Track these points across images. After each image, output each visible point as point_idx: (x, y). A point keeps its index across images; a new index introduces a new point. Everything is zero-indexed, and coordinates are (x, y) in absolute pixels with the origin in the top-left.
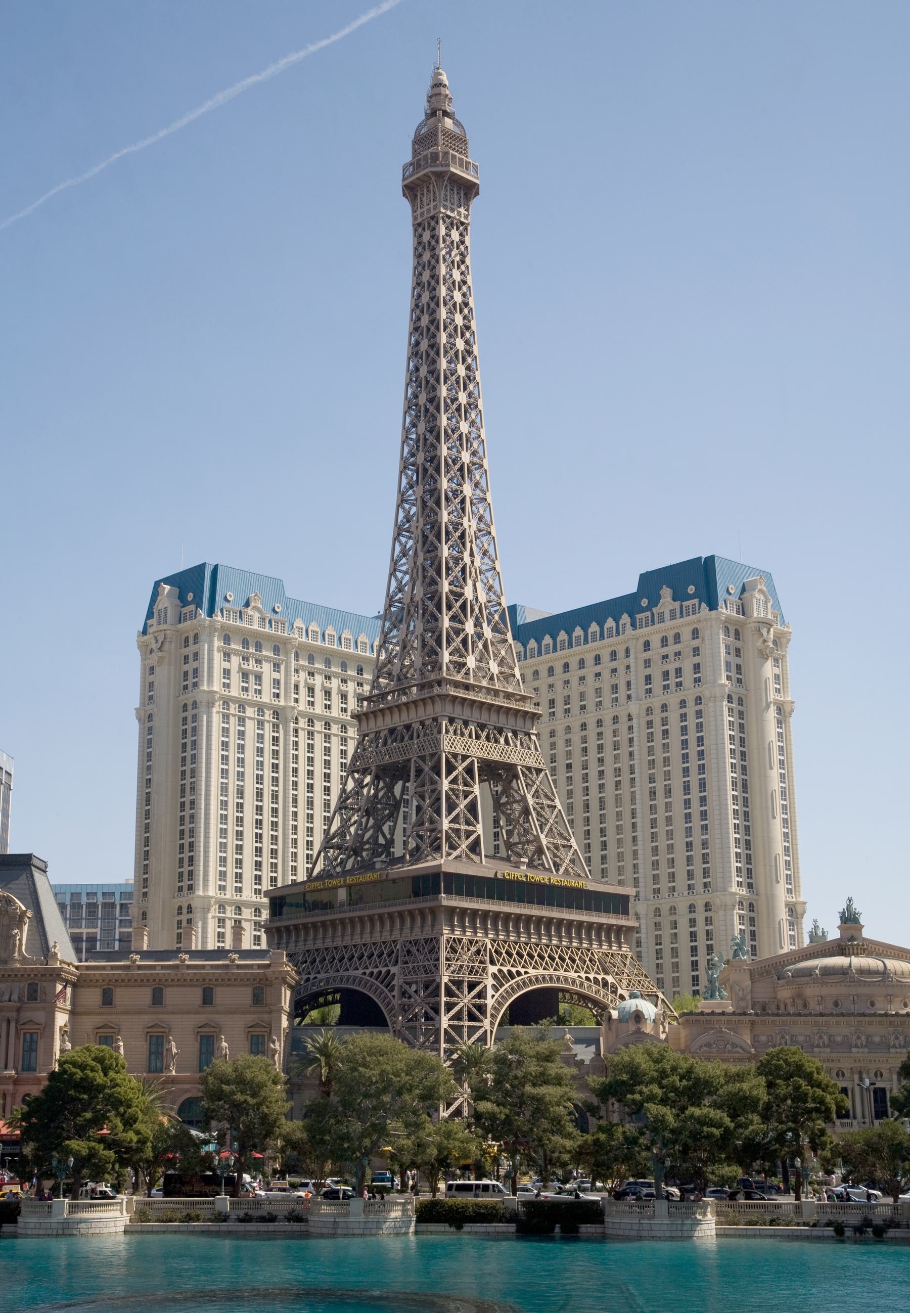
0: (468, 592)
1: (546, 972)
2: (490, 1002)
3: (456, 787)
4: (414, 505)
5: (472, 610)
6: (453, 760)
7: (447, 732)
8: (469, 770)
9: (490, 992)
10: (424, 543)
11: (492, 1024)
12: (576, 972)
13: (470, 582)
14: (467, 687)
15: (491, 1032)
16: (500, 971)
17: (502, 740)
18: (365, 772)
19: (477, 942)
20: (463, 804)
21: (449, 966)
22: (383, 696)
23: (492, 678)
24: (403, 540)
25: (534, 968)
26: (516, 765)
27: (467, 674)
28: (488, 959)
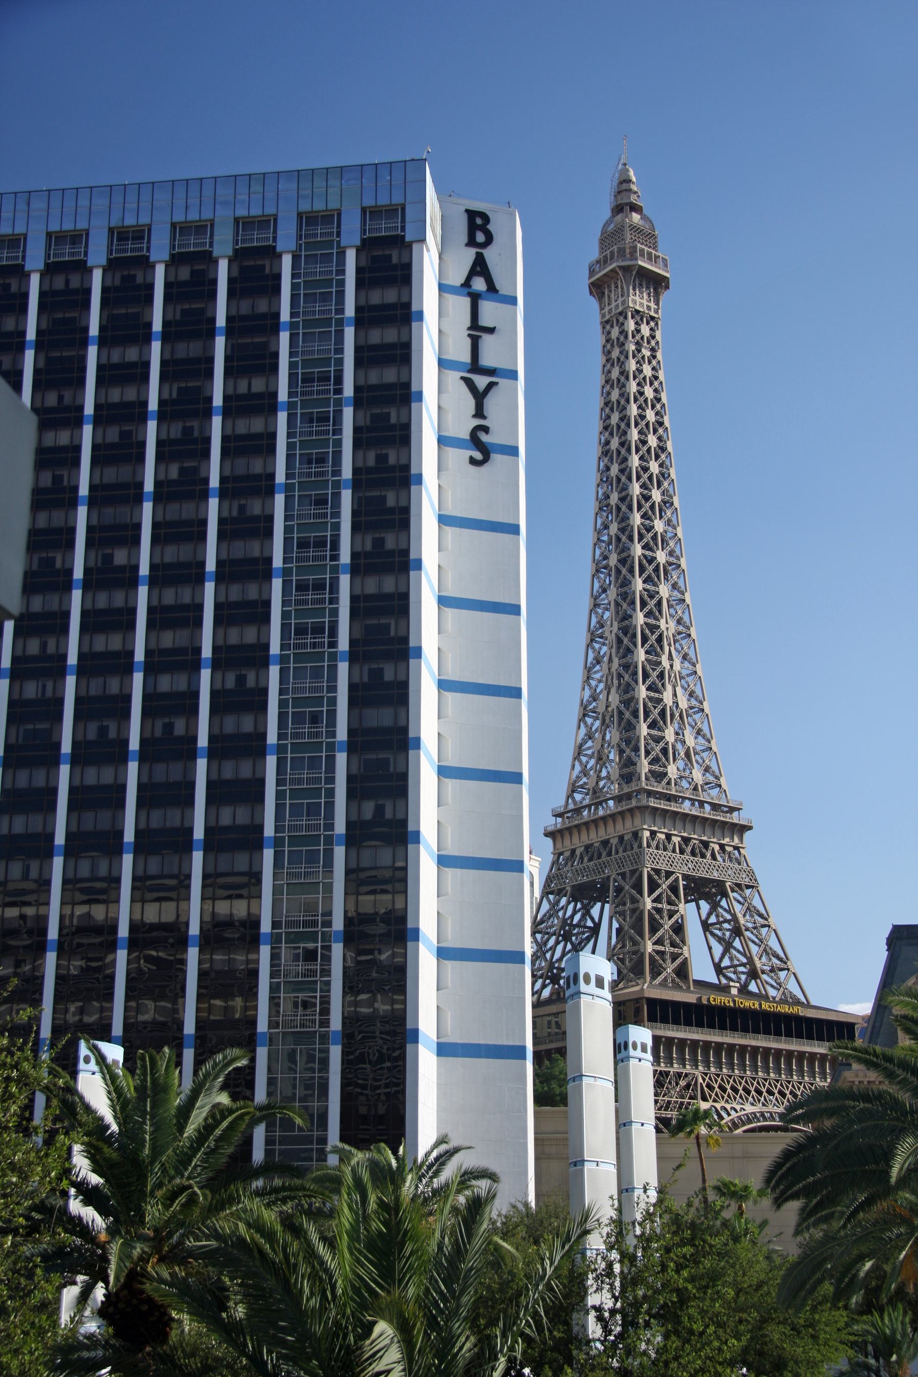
1: (764, 1109)
3: (660, 906)
4: (607, 609)
6: (656, 877)
7: (649, 846)
8: (674, 888)
10: (618, 648)
13: (669, 688)
14: (669, 798)
17: (708, 854)
18: (560, 893)
20: (668, 924)
22: (578, 811)
23: (695, 789)
24: (597, 646)
27: (669, 783)
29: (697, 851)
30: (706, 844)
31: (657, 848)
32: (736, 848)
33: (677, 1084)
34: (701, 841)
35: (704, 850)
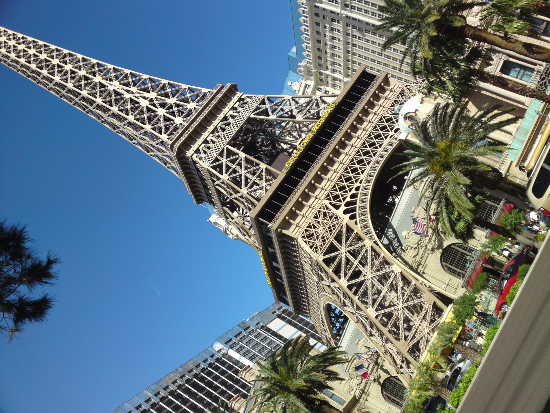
0: (144, 103)
2: (358, 229)
5: (154, 105)
7: (200, 159)
9: (351, 224)
11: (371, 238)
12: (386, 138)
13: (141, 100)
15: (375, 242)
16: (347, 204)
17: (231, 120)
19: (319, 212)
21: (316, 248)
25: (362, 172)
26: (249, 120)
28: (333, 210)
29: (224, 127)
30: (225, 118)
31: (205, 152)
32: (240, 100)
33: (318, 222)
34: (221, 121)
35: (227, 122)
